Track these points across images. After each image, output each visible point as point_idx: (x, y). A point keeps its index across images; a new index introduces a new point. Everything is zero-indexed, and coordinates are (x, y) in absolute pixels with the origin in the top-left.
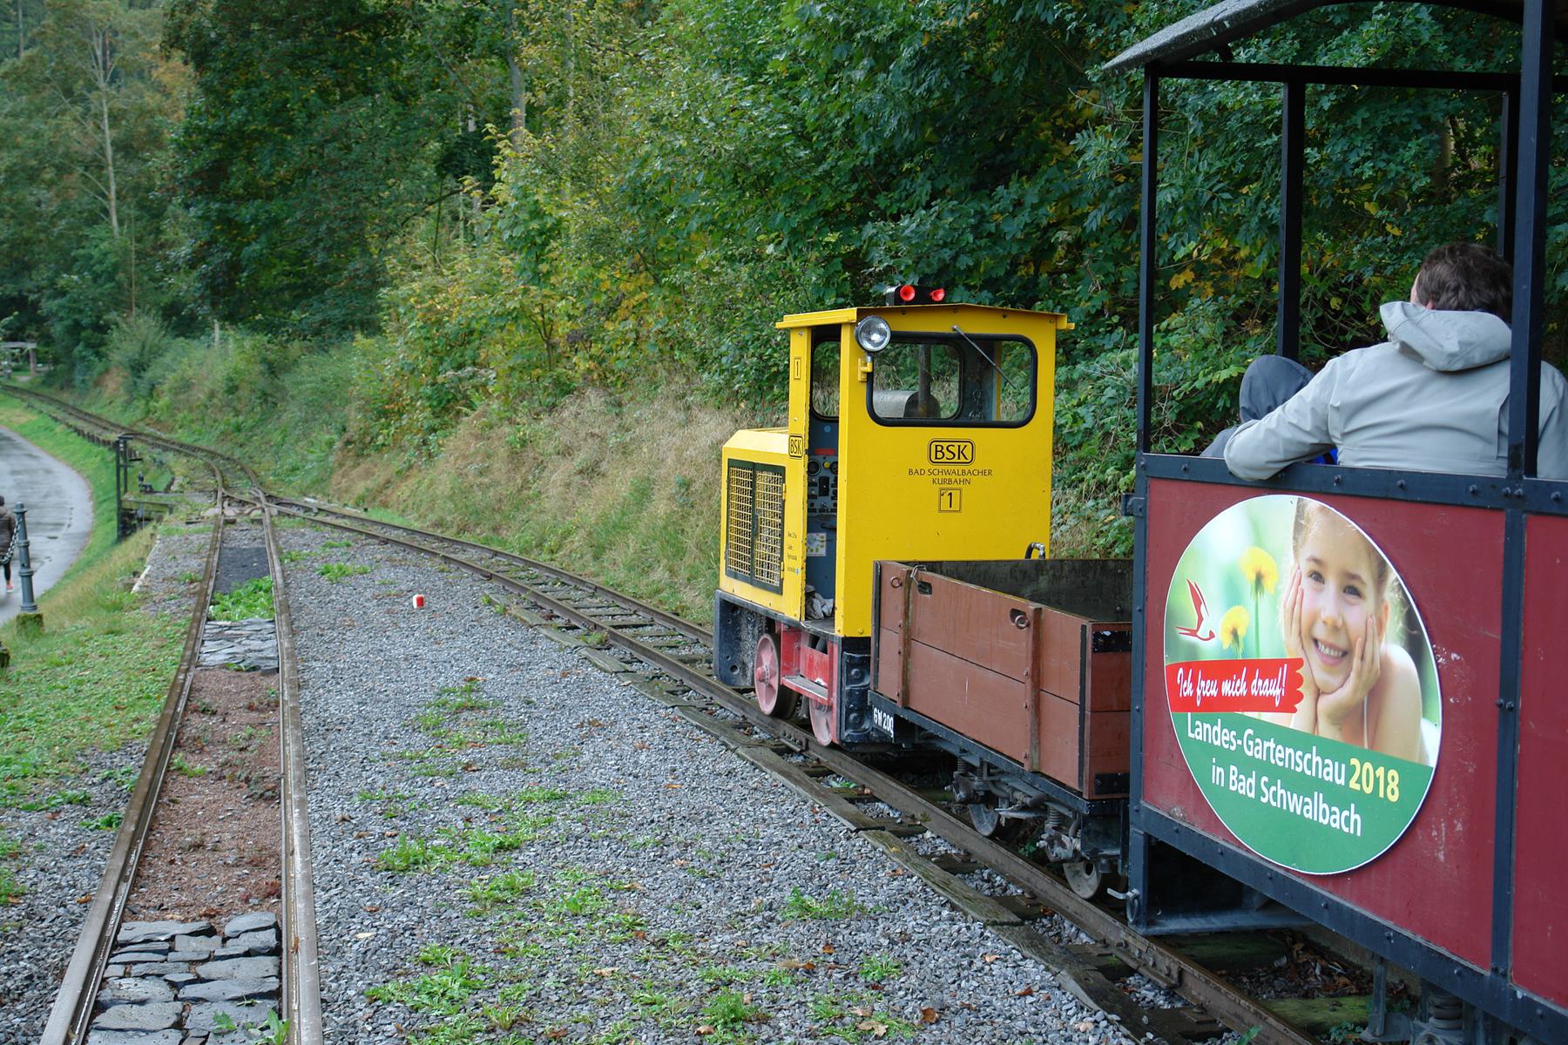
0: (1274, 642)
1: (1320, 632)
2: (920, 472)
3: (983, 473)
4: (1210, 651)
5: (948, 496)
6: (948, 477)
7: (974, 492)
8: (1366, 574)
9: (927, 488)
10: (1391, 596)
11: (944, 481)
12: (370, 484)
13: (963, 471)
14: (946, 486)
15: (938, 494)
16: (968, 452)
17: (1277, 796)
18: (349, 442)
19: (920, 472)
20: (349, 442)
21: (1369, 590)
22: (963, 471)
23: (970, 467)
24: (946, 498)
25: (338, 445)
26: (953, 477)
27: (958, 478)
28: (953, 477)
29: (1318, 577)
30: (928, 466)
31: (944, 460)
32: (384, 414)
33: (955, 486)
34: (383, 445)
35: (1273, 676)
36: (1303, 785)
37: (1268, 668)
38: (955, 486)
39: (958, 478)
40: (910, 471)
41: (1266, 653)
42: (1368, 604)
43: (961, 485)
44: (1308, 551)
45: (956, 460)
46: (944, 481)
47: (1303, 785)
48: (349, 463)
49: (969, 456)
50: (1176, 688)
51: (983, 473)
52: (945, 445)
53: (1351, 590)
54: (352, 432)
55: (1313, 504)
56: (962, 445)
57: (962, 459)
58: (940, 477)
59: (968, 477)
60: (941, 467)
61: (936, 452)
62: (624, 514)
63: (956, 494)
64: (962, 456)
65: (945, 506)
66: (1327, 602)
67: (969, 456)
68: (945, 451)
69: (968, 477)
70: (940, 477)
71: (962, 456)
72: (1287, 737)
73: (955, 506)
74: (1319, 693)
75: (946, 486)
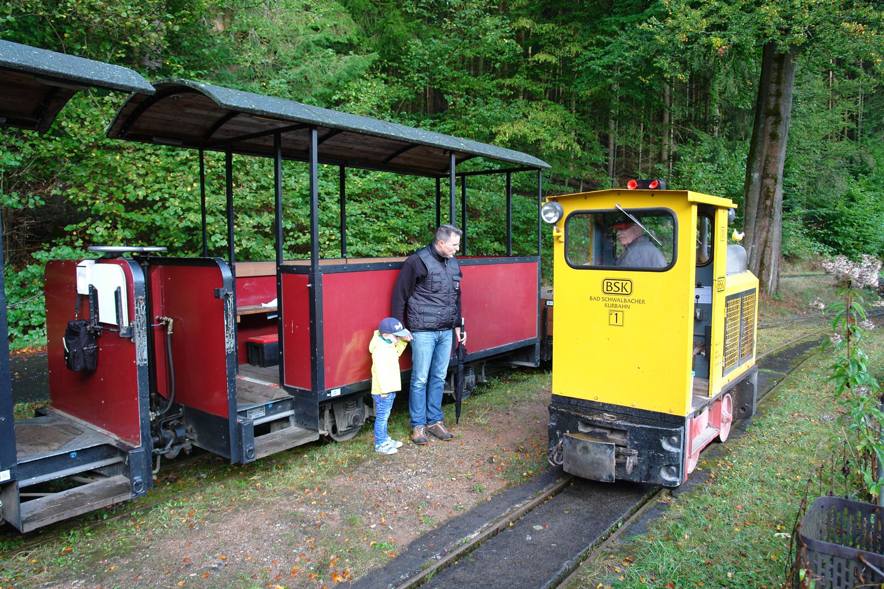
2: (597, 299)
3: (639, 301)
6: (615, 303)
7: (632, 314)
9: (601, 309)
11: (612, 305)
13: (625, 300)
14: (612, 309)
16: (628, 287)
19: (597, 299)
22: (625, 300)
23: (630, 297)
24: (613, 317)
26: (618, 303)
27: (621, 304)
28: (618, 303)
30: (602, 295)
31: (612, 292)
33: (620, 309)
38: (620, 309)
39: (621, 304)
40: (591, 298)
45: (620, 292)
46: (612, 305)
51: (639, 301)
52: (613, 282)
56: (624, 282)
57: (624, 292)
58: (610, 303)
59: (628, 304)
60: (610, 296)
61: (608, 287)
63: (620, 314)
64: (624, 290)
65: (613, 321)
68: (613, 286)
69: (628, 304)
70: (610, 303)
71: (624, 290)
73: (620, 322)
75: (612, 309)
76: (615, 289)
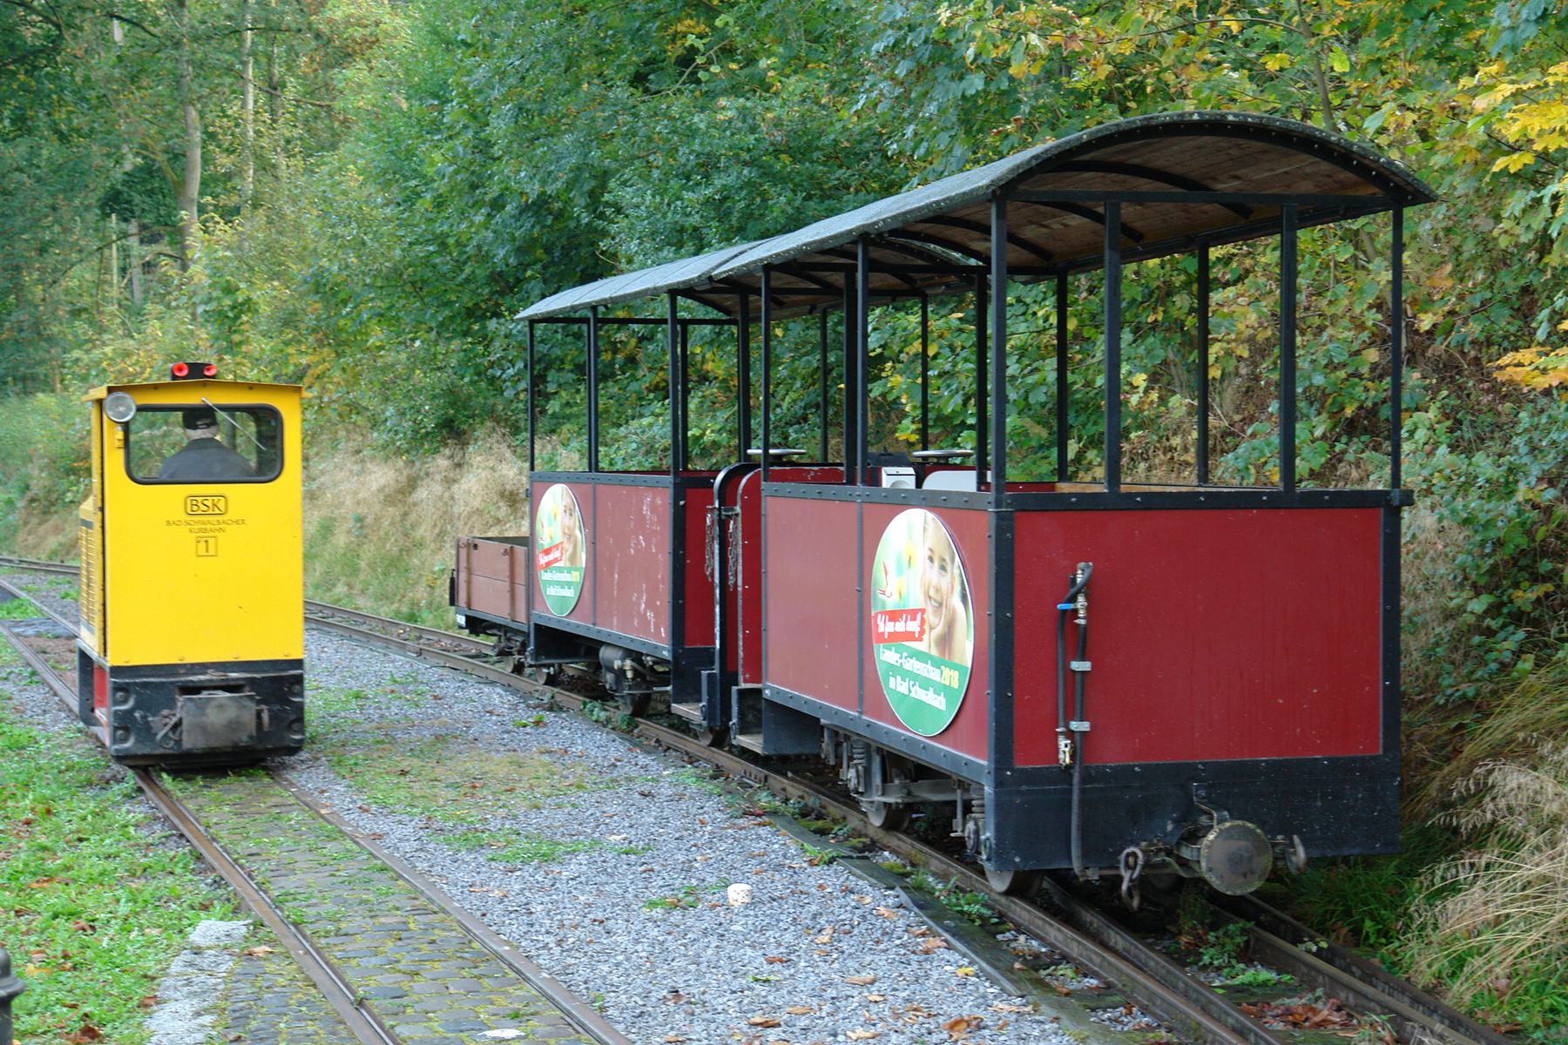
0: (916, 601)
1: (932, 593)
3: (237, 522)
4: (891, 604)
5: (205, 544)
8: (947, 558)
10: (956, 572)
11: (200, 530)
12: (61, 538)
15: (194, 542)
16: (221, 505)
17: (919, 694)
18: (33, 500)
20: (33, 500)
21: (949, 568)
24: (202, 546)
25: (20, 504)
26: (209, 527)
28: (209, 527)
29: (931, 559)
32: (70, 471)
33: (211, 534)
34: (72, 502)
35: (914, 619)
36: (926, 684)
37: (913, 614)
38: (211, 534)
41: (912, 606)
42: (949, 575)
43: (216, 534)
44: (928, 545)
46: (200, 530)
47: (926, 684)
48: (34, 521)
49: (223, 509)
50: (877, 626)
51: (237, 522)
52: (199, 499)
53: (943, 568)
54: (36, 489)
55: (930, 515)
57: (217, 511)
58: (197, 526)
59: (222, 526)
61: (193, 508)
62: (312, 547)
63: (211, 541)
64: (216, 510)
66: (933, 573)
67: (223, 509)
69: (222, 526)
70: (197, 526)
71: (216, 510)
72: (921, 657)
73: (212, 552)
74: (931, 628)
76: (205, 508)
